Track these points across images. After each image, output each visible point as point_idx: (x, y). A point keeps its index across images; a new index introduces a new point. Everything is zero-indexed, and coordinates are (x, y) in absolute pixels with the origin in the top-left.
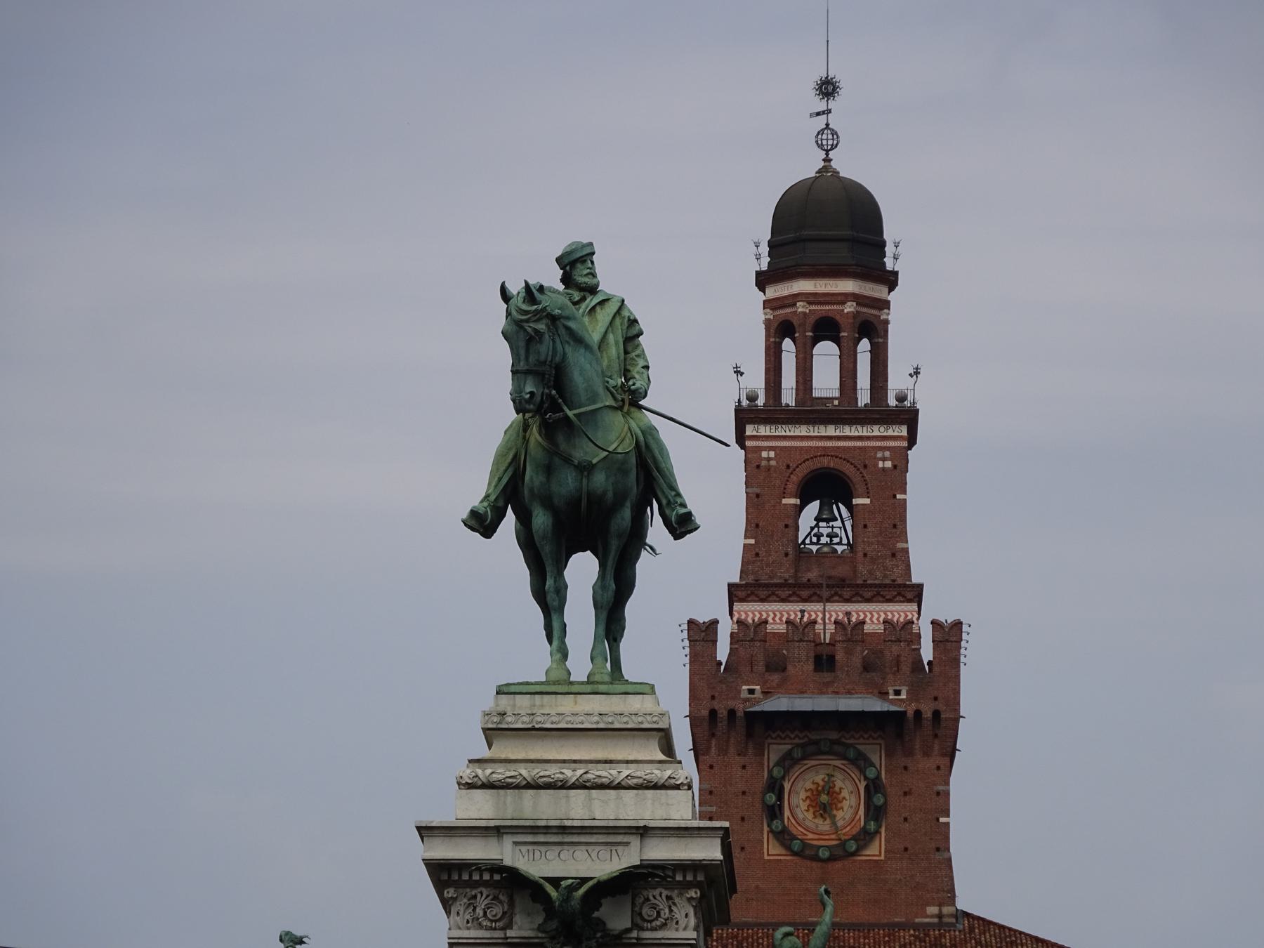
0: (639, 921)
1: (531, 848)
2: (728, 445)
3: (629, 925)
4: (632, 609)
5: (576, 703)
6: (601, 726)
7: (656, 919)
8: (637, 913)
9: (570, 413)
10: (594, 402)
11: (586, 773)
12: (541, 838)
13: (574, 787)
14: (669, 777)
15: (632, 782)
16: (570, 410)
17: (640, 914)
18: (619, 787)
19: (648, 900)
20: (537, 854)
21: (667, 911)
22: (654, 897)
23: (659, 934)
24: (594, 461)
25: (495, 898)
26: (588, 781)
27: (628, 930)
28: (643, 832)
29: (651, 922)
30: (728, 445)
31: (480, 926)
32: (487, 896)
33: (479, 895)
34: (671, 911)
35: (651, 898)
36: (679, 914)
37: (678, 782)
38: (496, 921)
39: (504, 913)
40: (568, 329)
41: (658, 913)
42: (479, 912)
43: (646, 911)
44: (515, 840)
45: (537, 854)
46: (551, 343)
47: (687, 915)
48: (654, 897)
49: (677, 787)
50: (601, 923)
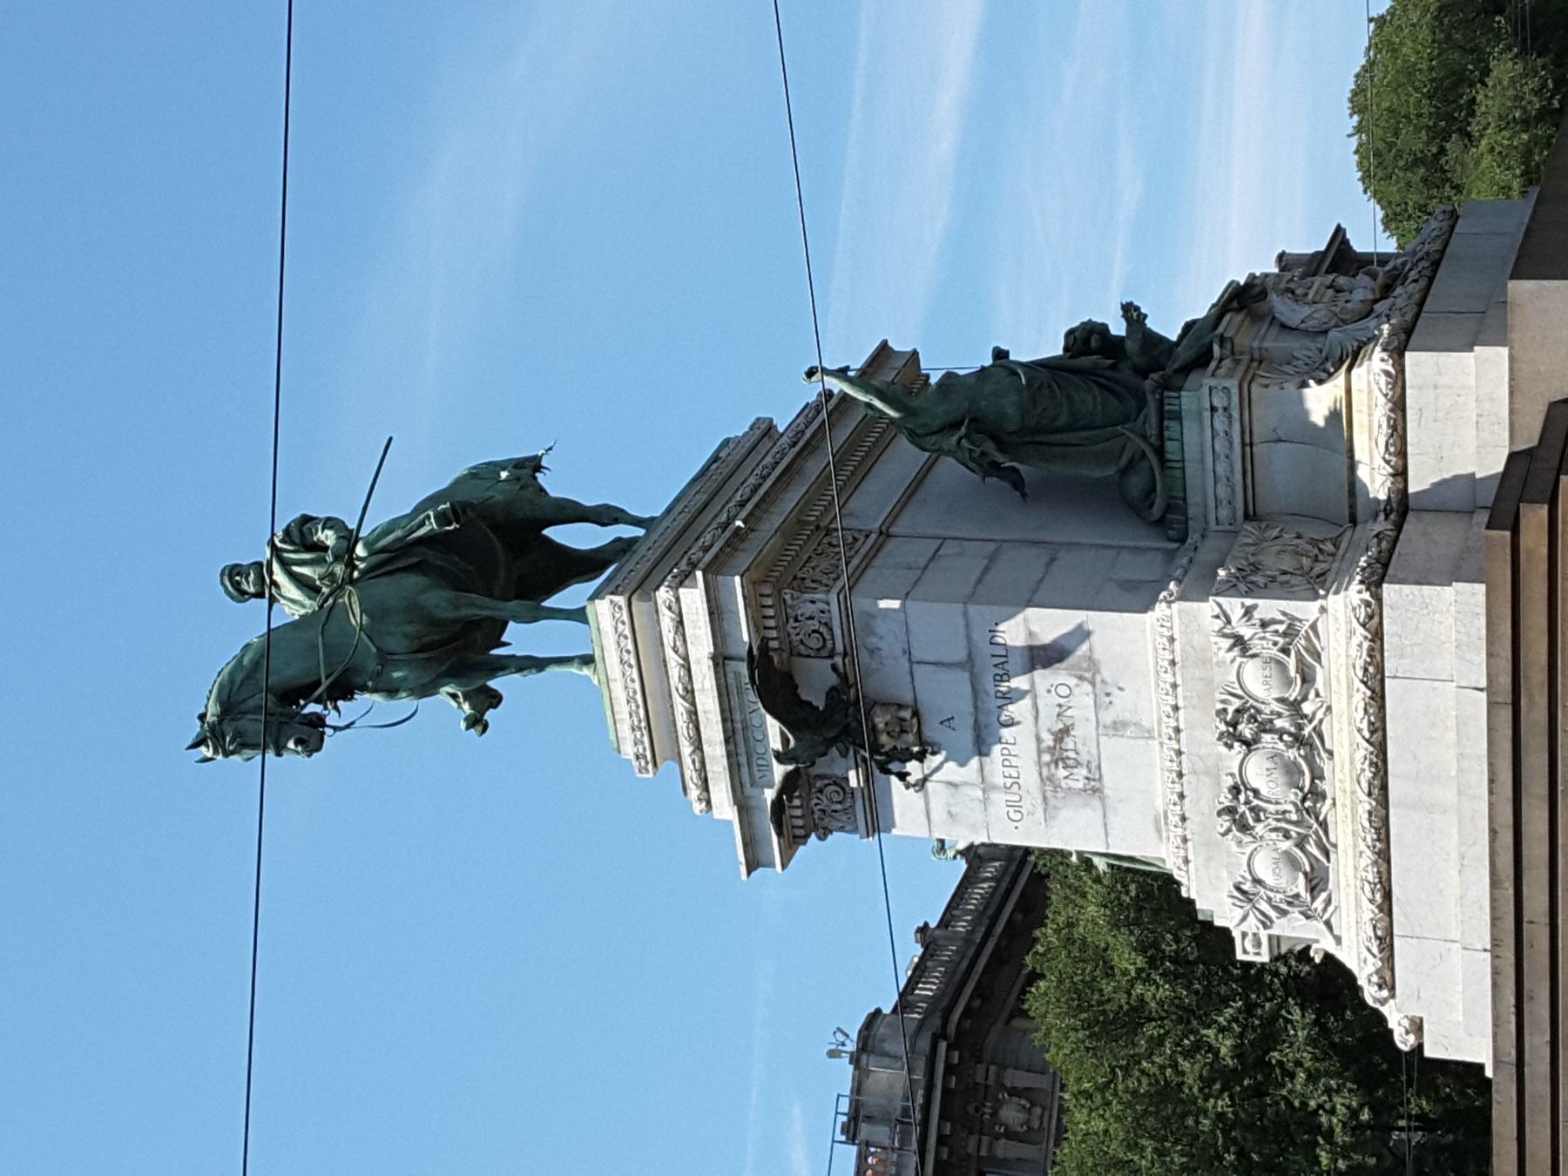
0: (825, 653)
1: (755, 768)
2: (390, 439)
3: (829, 662)
4: (589, 501)
5: (615, 680)
6: (633, 662)
7: (821, 634)
8: (818, 654)
9: (325, 684)
10: (318, 647)
11: (677, 690)
12: (743, 760)
13: (693, 704)
14: (670, 608)
15: (681, 650)
16: (318, 683)
17: (818, 650)
18: (686, 659)
19: (801, 641)
20: (760, 762)
21: (811, 622)
22: (798, 634)
23: (837, 632)
24: (374, 650)
25: (821, 791)
26: (685, 689)
27: (834, 668)
28: (720, 660)
29: (824, 640)
30: (390, 439)
31: (853, 806)
32: (819, 798)
33: (819, 807)
34: (811, 618)
35: (798, 638)
36: (809, 609)
37: (674, 600)
38: (844, 792)
39: (835, 783)
40: (242, 683)
41: (814, 631)
42: (839, 807)
43: (814, 643)
44: (749, 785)
45: (760, 762)
46: (249, 716)
47: (813, 602)
48: (798, 634)
49: (678, 599)
50: (832, 693)
